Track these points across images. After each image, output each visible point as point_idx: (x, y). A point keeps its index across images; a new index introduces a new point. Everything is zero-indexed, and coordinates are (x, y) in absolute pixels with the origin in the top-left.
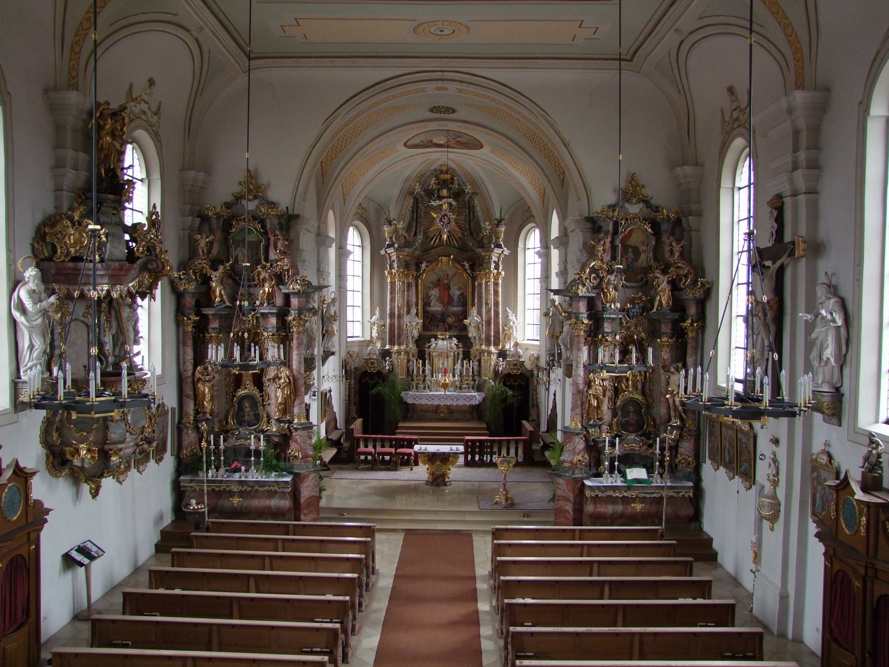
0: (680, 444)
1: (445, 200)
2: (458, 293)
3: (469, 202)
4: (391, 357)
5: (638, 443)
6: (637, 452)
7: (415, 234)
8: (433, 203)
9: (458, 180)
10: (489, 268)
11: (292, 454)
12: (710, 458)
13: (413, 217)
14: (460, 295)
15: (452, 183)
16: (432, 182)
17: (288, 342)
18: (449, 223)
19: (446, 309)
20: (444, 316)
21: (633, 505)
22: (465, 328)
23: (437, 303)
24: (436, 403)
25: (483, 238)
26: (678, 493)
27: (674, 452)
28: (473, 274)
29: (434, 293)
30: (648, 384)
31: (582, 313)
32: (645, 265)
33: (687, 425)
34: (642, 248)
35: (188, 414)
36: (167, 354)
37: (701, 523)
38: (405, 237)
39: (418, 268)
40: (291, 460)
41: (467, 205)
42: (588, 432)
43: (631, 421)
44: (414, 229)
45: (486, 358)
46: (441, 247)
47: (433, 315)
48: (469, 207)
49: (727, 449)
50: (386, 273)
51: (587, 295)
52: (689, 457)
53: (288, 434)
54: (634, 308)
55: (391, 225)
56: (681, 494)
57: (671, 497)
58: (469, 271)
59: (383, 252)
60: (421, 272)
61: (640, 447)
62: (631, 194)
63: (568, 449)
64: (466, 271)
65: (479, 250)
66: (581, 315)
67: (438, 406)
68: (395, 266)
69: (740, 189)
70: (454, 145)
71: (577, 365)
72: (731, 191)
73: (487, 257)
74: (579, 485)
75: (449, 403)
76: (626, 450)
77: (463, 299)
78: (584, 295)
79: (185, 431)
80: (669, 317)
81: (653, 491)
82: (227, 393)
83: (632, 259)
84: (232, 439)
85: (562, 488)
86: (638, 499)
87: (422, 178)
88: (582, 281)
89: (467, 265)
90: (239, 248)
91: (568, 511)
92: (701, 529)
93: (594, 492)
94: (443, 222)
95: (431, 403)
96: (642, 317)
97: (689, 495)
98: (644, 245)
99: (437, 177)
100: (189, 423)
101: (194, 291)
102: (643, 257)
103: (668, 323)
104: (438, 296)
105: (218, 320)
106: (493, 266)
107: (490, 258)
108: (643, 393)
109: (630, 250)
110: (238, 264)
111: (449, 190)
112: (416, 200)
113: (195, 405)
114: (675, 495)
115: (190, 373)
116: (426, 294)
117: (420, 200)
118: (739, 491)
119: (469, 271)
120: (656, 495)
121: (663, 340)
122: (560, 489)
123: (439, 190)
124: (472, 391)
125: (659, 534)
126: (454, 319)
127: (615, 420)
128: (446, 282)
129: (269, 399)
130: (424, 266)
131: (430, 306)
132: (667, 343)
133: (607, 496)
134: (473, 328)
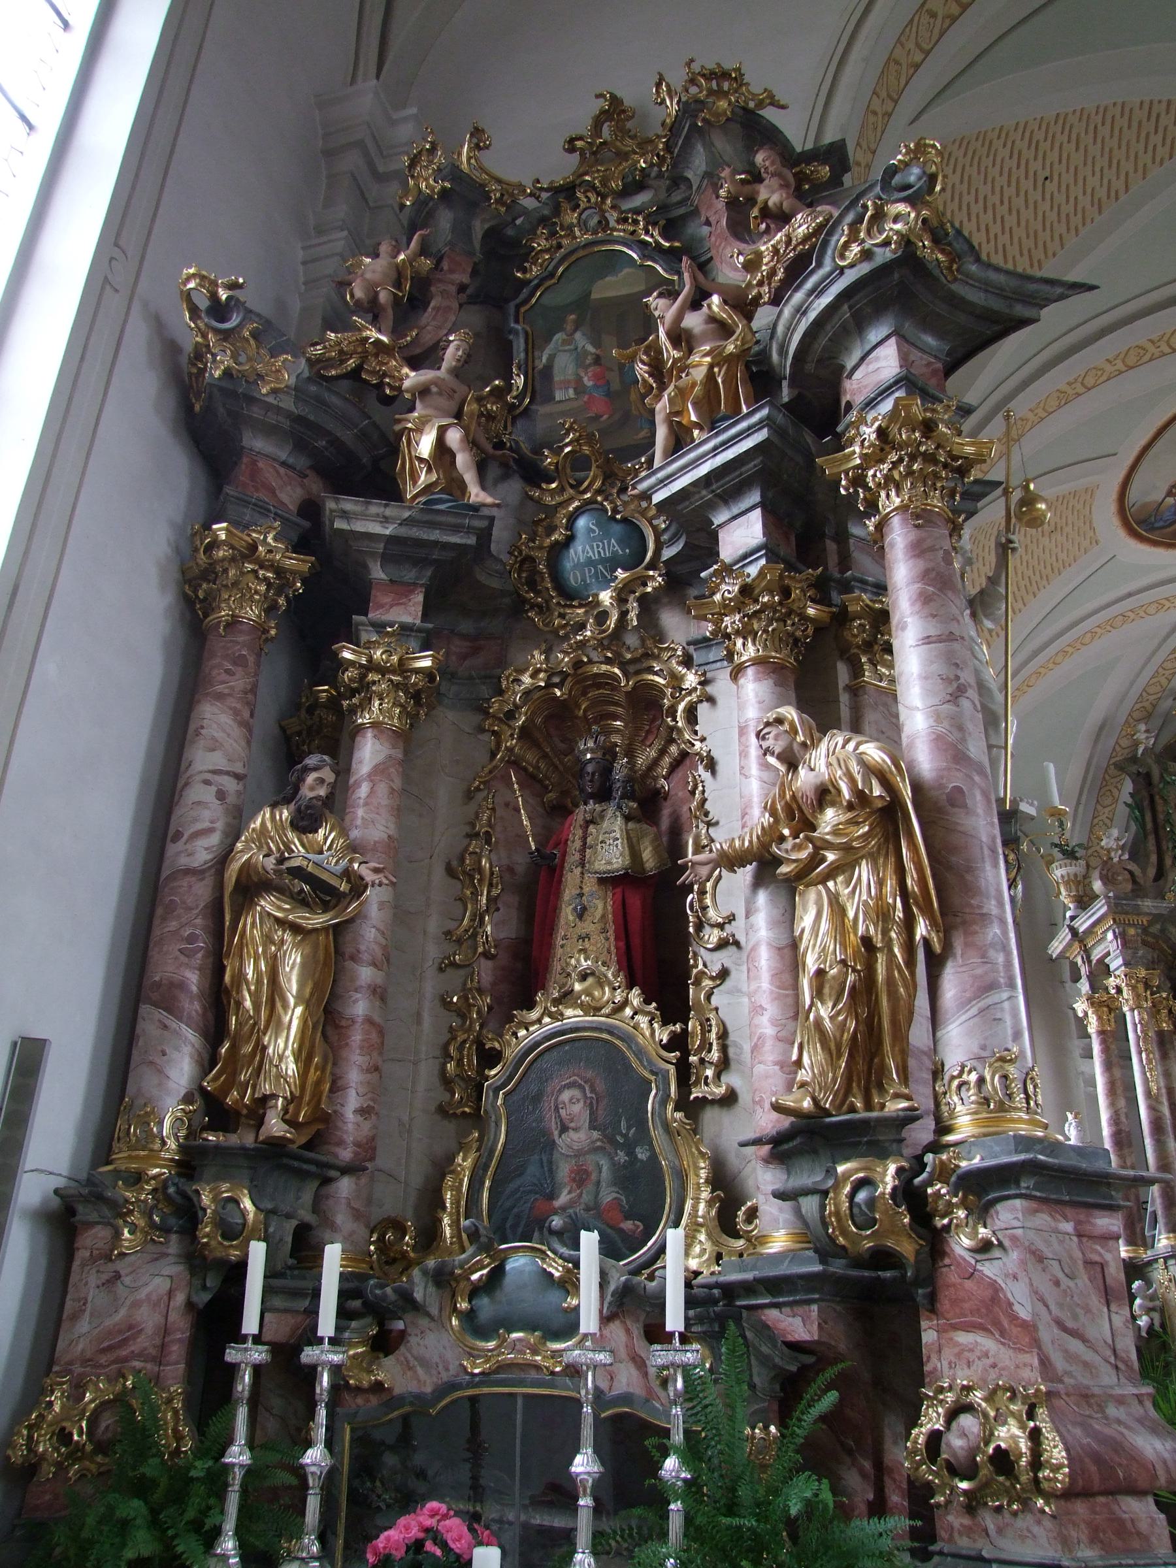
4: (1148, 1283)
11: (956, 1443)
13: (1142, 825)
17: (843, 673)
35: (153, 1116)
36: (48, 667)
38: (1131, 873)
40: (955, 1519)
44: (1154, 858)
50: (1081, 1007)
53: (907, 1248)
55: (1077, 859)
59: (1056, 947)
68: (1116, 963)
79: (93, 1239)
82: (445, 1048)
84: (440, 1323)
90: (559, 337)
100: (136, 1179)
101: (288, 403)
105: (420, 598)
110: (550, 398)
112: (1144, 781)
113: (207, 1061)
115: (202, 852)
129: (724, 1064)
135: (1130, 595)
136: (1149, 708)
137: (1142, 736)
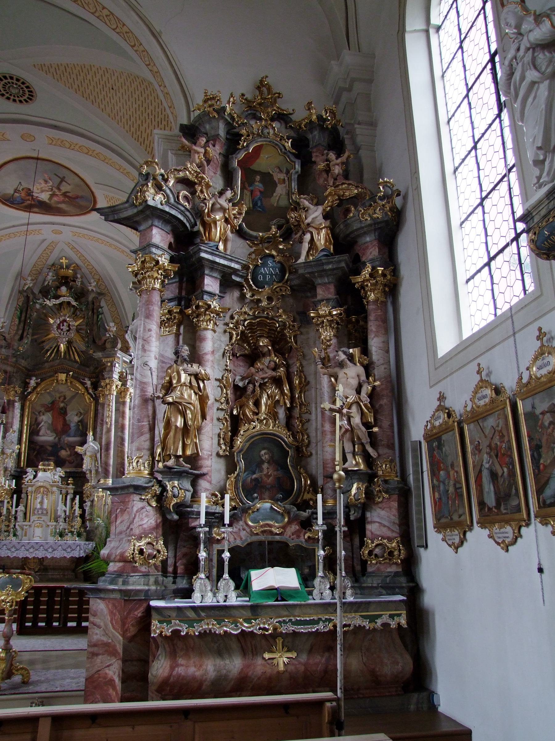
0: (368, 515)
1: (62, 299)
2: (76, 419)
3: (93, 304)
5: (279, 517)
6: (278, 538)
7: (21, 338)
8: (48, 302)
9: (82, 277)
10: (111, 377)
12: (439, 527)
13: (20, 318)
14: (79, 422)
15: (74, 281)
16: (49, 278)
18: (68, 331)
19: (59, 439)
20: (56, 448)
21: (267, 656)
22: (80, 458)
23: (49, 432)
24: (21, 554)
25: (105, 341)
26: (373, 619)
27: (357, 541)
28: (94, 394)
29: (46, 419)
30: (296, 412)
31: (157, 247)
32: (284, 202)
33: (380, 473)
34: (278, 176)
37: (431, 694)
39: (26, 385)
41: (90, 306)
42: (164, 489)
43: (265, 479)
45: (101, 494)
46: (58, 361)
47: (42, 447)
48: (93, 310)
49: (485, 474)
51: (167, 209)
52: (390, 540)
54: (264, 265)
56: (379, 622)
57: (359, 629)
58: (91, 391)
60: (30, 390)
61: (284, 527)
62: (260, 104)
63: (118, 530)
64: (89, 393)
65: (98, 355)
66: (154, 250)
67: (27, 558)
69: (438, 29)
70: (63, 206)
71: (143, 346)
72: (423, 36)
73: (109, 364)
74: (139, 613)
75: (40, 554)
76: (252, 534)
77: (83, 427)
78: (159, 206)
80: (330, 266)
81: (316, 618)
83: (260, 192)
85: (102, 624)
86: (279, 641)
87: (37, 273)
88: (154, 179)
89: (88, 383)
91: (111, 682)
92: (433, 708)
93: (169, 622)
94: (62, 330)
95: (15, 555)
96: (281, 284)
97: (399, 624)
98: (281, 171)
99: (57, 274)
102: (280, 190)
103: (329, 283)
104: (50, 422)
106: (116, 376)
107: (113, 366)
108: (289, 425)
109: (258, 178)
111: (70, 288)
114: (366, 624)
116: (34, 420)
117: (31, 298)
118: (545, 567)
119: (91, 391)
120: (321, 627)
121: (321, 312)
122: (99, 627)
123: (58, 288)
124: (77, 539)
125: (326, 718)
126: (69, 453)
127: (233, 477)
128: (62, 405)
130: (33, 382)
131: (38, 435)
132: (329, 318)
133: (204, 635)
134: (89, 459)
135: (14, 226)
136: (39, 270)
137: (29, 282)
